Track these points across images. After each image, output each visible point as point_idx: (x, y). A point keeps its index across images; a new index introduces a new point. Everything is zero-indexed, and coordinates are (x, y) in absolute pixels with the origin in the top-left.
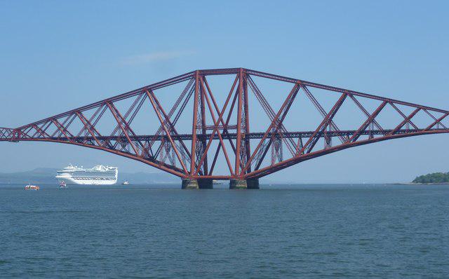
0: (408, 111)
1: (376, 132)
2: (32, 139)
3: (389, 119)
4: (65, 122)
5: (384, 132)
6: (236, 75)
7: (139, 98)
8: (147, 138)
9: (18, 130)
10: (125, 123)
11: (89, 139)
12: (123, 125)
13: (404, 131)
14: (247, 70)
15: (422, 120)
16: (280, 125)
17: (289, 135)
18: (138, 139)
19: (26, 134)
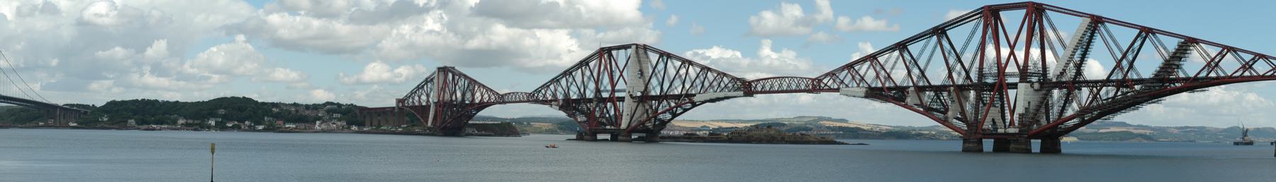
0: (1213, 52)
1: (1178, 80)
2: (831, 90)
3: (1193, 64)
4: (859, 70)
5: (1187, 79)
6: (1024, 11)
7: (928, 43)
8: (938, 89)
9: (819, 80)
10: (919, 68)
11: (881, 89)
12: (916, 71)
13: (1213, 79)
14: (1041, 5)
15: (1230, 65)
16: (1079, 72)
17: (1088, 83)
18: (931, 87)
19: (826, 85)
